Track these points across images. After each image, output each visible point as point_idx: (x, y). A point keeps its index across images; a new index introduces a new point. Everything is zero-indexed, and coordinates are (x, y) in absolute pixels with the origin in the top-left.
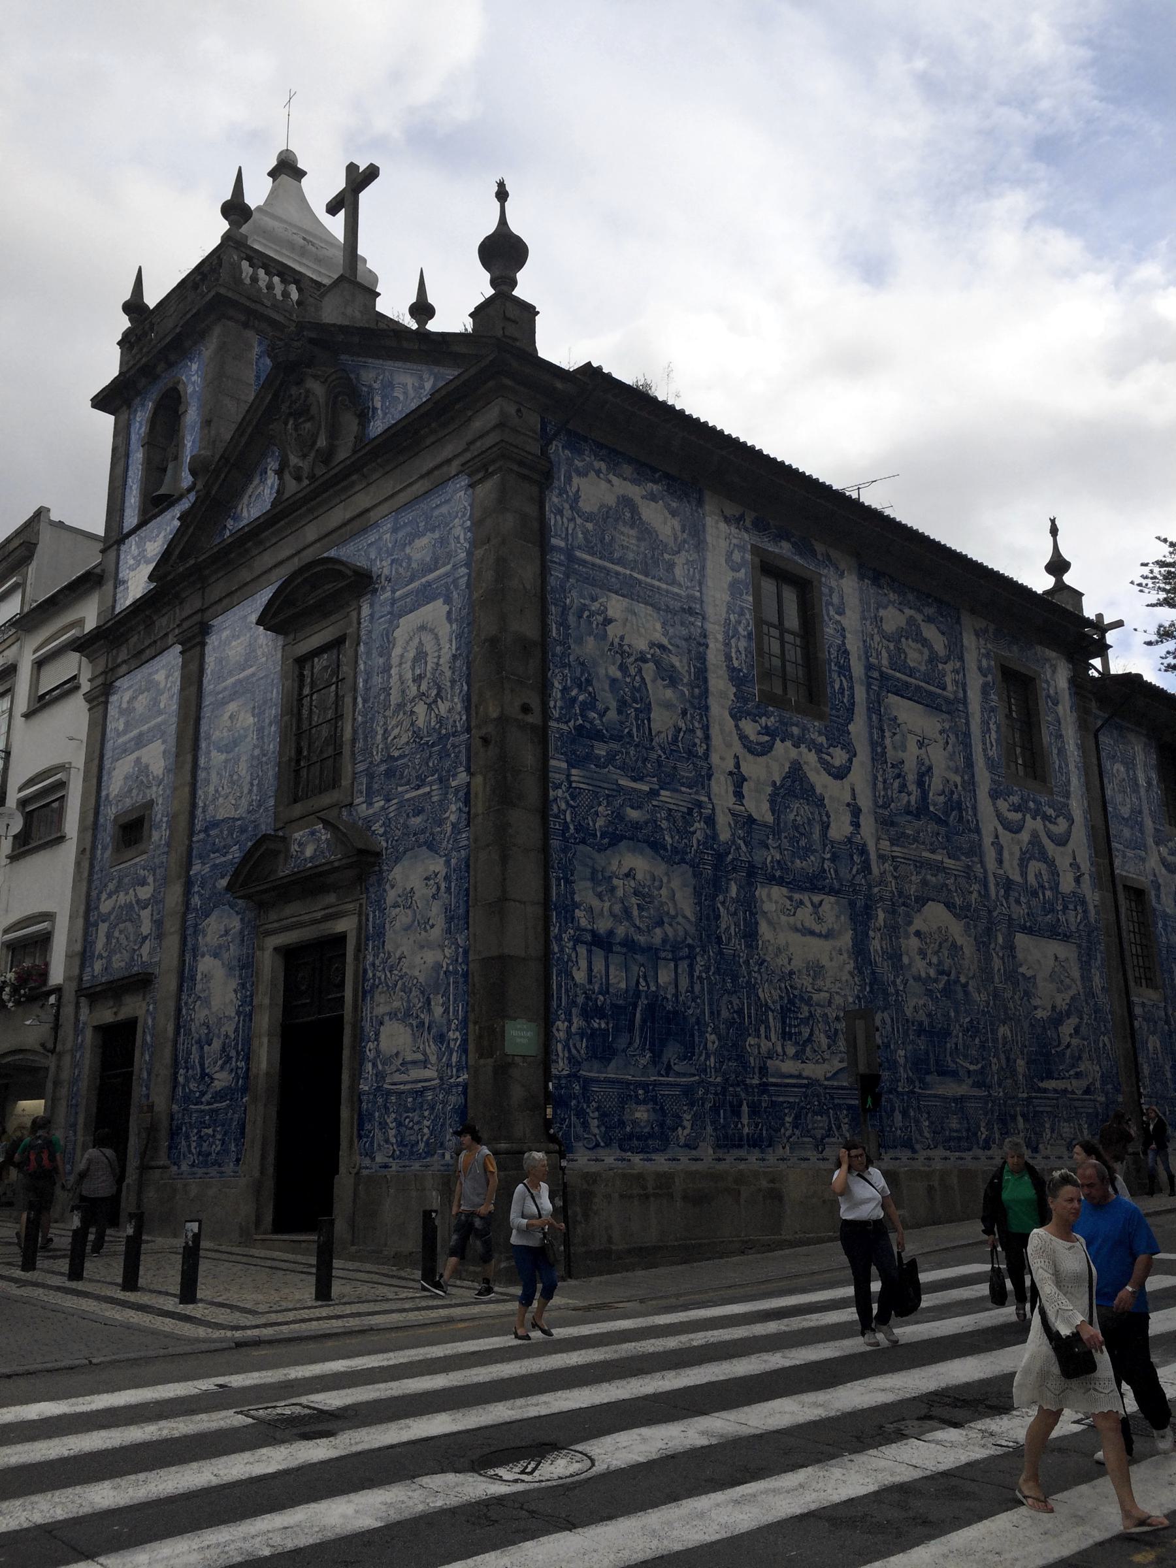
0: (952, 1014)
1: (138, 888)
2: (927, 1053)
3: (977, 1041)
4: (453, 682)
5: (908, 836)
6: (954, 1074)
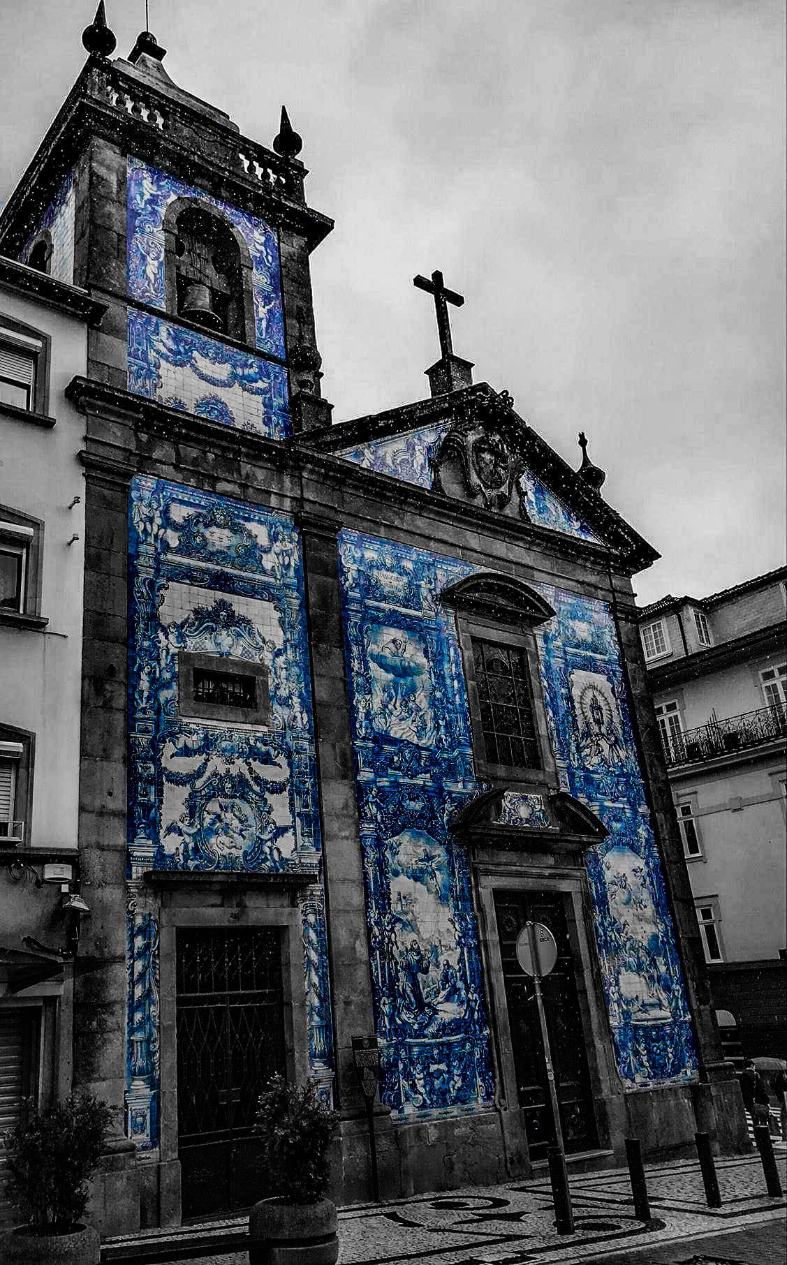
1: (256, 765)
4: (626, 741)
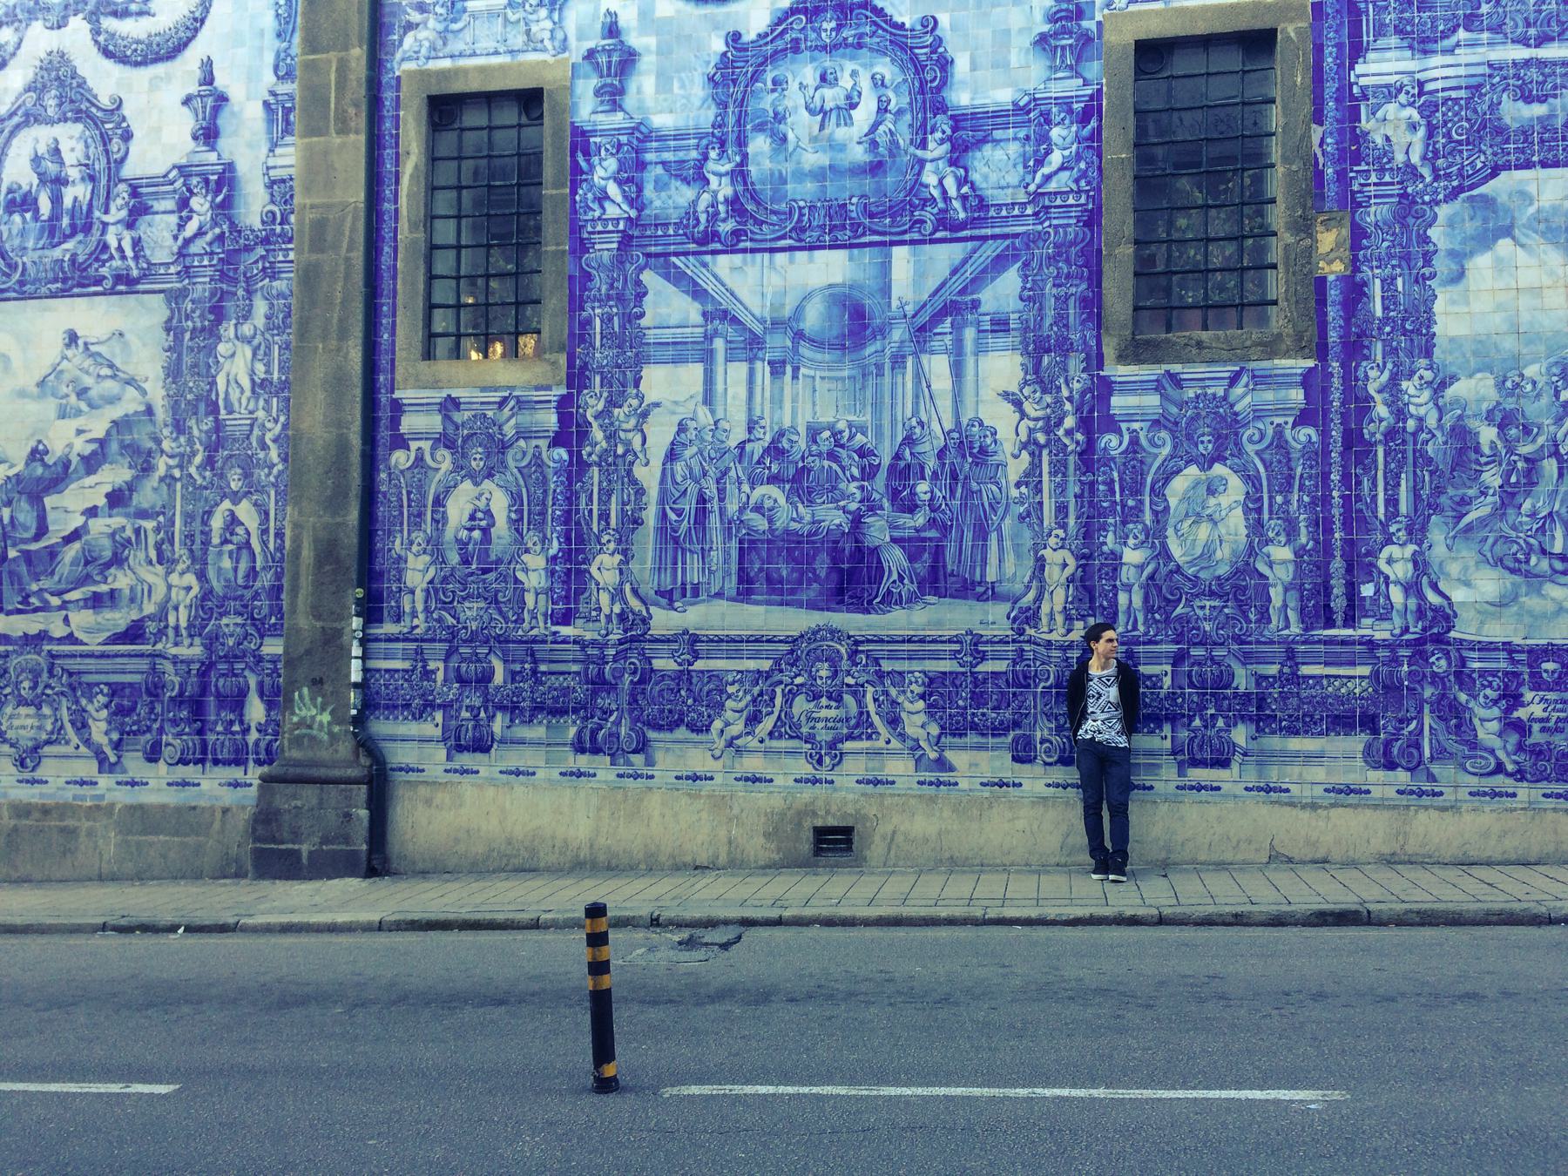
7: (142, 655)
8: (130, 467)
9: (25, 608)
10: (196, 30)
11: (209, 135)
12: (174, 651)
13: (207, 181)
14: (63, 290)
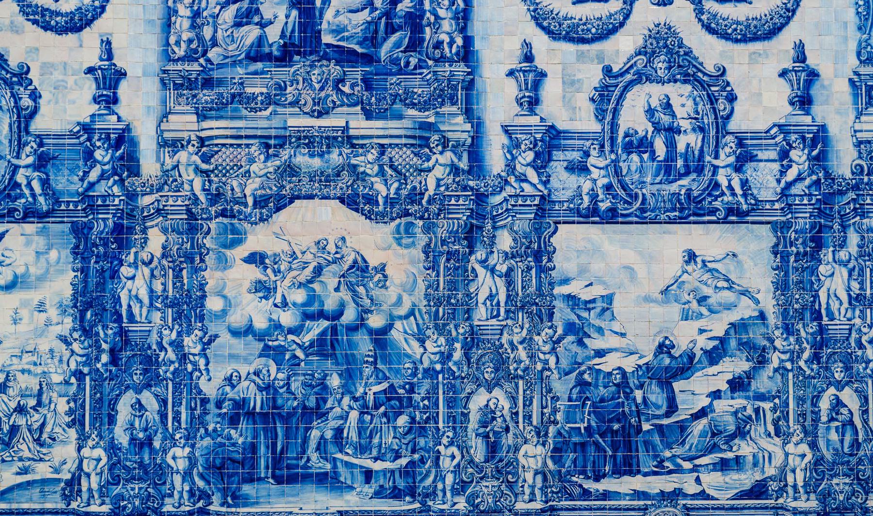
0: (335, 381)
2: (254, 448)
3: (402, 421)
5: (254, 97)
6: (323, 480)
7: (766, 508)
8: (748, 360)
9: (660, 470)
10: (789, 19)
11: (804, 102)
12: (794, 504)
13: (804, 138)
14: (680, 218)
